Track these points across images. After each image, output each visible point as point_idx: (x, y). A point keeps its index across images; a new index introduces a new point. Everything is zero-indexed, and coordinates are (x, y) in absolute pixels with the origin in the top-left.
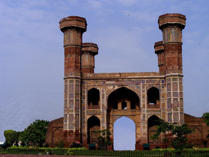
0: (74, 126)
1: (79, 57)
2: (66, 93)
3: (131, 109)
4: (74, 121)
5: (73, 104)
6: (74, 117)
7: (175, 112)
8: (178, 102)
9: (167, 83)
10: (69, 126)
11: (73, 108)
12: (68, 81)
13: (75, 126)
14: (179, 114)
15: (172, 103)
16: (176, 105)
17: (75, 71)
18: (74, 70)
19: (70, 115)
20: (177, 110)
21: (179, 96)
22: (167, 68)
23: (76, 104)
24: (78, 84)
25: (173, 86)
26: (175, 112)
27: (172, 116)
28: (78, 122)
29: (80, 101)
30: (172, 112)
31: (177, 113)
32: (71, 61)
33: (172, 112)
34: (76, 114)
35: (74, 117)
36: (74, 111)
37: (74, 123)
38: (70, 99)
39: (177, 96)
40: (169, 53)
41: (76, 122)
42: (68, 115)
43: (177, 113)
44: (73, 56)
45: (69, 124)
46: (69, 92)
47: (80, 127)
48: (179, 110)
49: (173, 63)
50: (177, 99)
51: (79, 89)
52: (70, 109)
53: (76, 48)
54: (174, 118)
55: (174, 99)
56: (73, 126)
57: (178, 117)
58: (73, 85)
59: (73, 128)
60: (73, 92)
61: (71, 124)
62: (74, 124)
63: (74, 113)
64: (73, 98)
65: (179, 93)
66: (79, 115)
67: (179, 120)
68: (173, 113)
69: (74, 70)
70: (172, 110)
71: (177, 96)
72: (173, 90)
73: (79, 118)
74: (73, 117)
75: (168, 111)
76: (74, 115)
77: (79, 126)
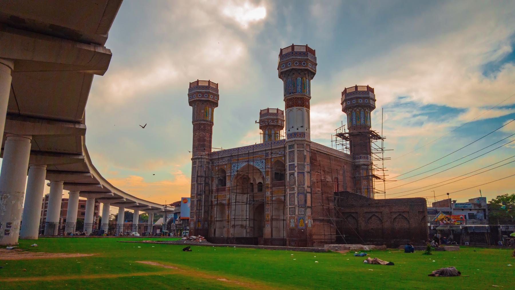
4: (195, 209)
8: (294, 178)
14: (296, 195)
20: (294, 188)
21: (296, 169)
23: (198, 189)
25: (289, 155)
31: (294, 194)
43: (294, 194)
48: (296, 189)
50: (293, 174)
63: (195, 200)
65: (296, 165)
67: (296, 203)
71: (294, 170)
76: (195, 203)
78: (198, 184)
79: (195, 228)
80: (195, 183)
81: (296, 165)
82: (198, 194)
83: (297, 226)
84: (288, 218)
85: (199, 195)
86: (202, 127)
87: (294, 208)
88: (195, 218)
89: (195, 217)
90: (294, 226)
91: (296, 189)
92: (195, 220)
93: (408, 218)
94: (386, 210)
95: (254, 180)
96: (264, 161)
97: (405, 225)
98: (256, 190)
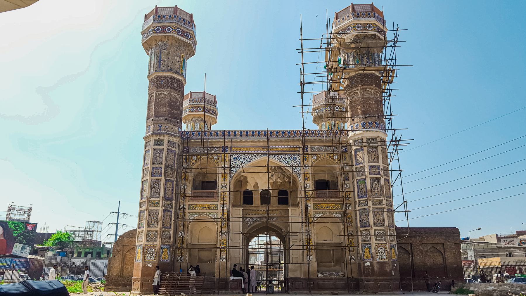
0: (158, 236)
1: (178, 97)
2: (146, 167)
3: (279, 204)
4: (160, 224)
5: (159, 188)
6: (160, 216)
7: (376, 206)
8: (380, 185)
9: (353, 148)
10: (147, 236)
11: (159, 197)
12: (152, 143)
13: (162, 237)
15: (369, 187)
16: (377, 191)
17: (167, 121)
18: (166, 119)
19: (150, 212)
20: (380, 202)
21: (382, 173)
22: (353, 120)
23: (165, 189)
24: (172, 149)
26: (376, 206)
27: (371, 214)
28: (168, 228)
29: (175, 183)
30: (370, 207)
32: (160, 104)
33: (370, 207)
34: (164, 211)
35: (160, 216)
36: (161, 203)
37: (158, 229)
38: (153, 178)
39: (379, 174)
40: (358, 90)
41: (165, 227)
42: (146, 213)
44: (165, 93)
45: (148, 231)
46: (153, 164)
47: (172, 240)
49: (367, 108)
50: (378, 180)
51: (174, 158)
52: (151, 199)
53: (171, 78)
54: (374, 220)
55: (373, 181)
56: (157, 237)
57: (384, 217)
58: (161, 150)
59: (156, 241)
60: (161, 163)
61: (153, 231)
62: (159, 232)
63: (160, 208)
64: (160, 176)
66: (171, 213)
68: (371, 209)
69: (166, 119)
70: (370, 203)
71: (379, 174)
72: (369, 162)
73: (171, 220)
74: (157, 216)
75: (359, 205)
76: (160, 214)
77: (170, 237)
78: (166, 181)
79: (159, 260)
80: (162, 178)
81: (381, 167)
82: (166, 198)
83: (389, 257)
84: (373, 246)
85: (167, 199)
86: (176, 84)
87: (384, 230)
88: (158, 243)
89: (159, 240)
90: (385, 257)
91: (384, 202)
92: (159, 246)
93: (443, 252)
94: (417, 242)
95: (256, 185)
96: (299, 158)
97: (439, 260)
98: (257, 201)
